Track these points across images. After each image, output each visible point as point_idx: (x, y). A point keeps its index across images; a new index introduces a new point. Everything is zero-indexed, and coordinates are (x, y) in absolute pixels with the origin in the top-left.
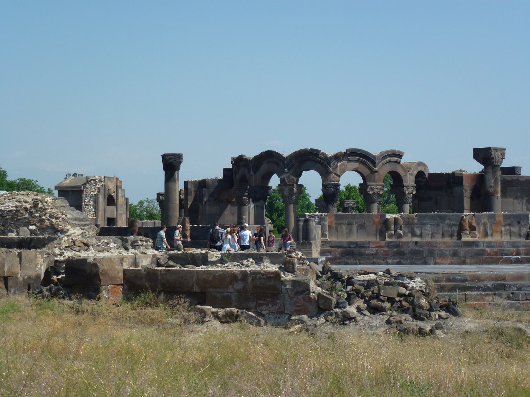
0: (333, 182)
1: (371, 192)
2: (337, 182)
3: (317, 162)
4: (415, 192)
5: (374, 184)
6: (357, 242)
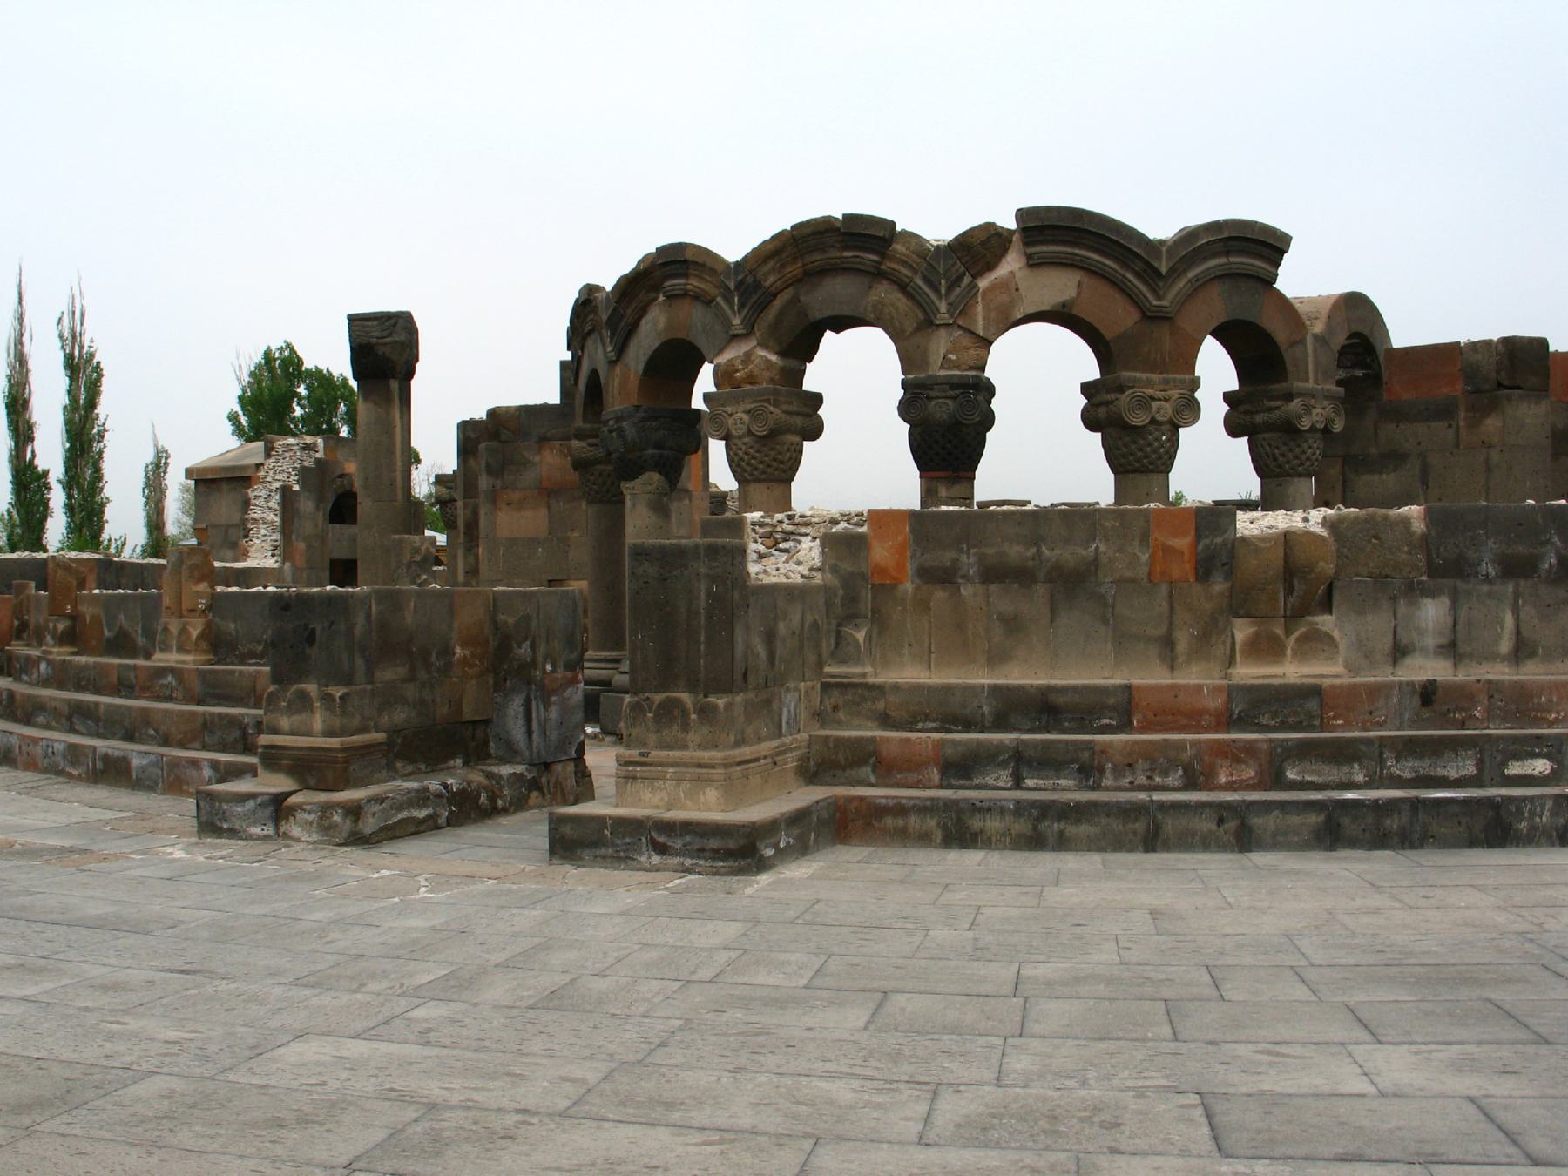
0: (957, 367)
1: (1139, 419)
2: (971, 368)
3: (878, 274)
4: (1338, 426)
5: (1155, 377)
6: (1050, 689)
